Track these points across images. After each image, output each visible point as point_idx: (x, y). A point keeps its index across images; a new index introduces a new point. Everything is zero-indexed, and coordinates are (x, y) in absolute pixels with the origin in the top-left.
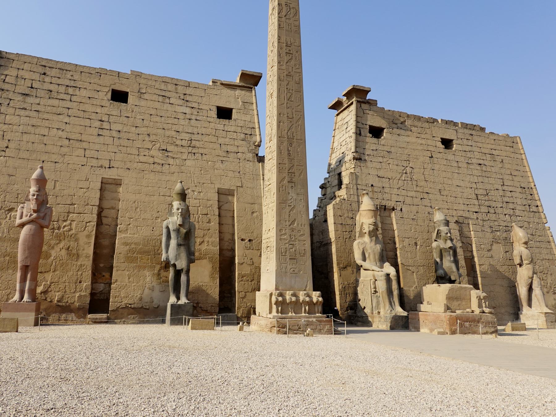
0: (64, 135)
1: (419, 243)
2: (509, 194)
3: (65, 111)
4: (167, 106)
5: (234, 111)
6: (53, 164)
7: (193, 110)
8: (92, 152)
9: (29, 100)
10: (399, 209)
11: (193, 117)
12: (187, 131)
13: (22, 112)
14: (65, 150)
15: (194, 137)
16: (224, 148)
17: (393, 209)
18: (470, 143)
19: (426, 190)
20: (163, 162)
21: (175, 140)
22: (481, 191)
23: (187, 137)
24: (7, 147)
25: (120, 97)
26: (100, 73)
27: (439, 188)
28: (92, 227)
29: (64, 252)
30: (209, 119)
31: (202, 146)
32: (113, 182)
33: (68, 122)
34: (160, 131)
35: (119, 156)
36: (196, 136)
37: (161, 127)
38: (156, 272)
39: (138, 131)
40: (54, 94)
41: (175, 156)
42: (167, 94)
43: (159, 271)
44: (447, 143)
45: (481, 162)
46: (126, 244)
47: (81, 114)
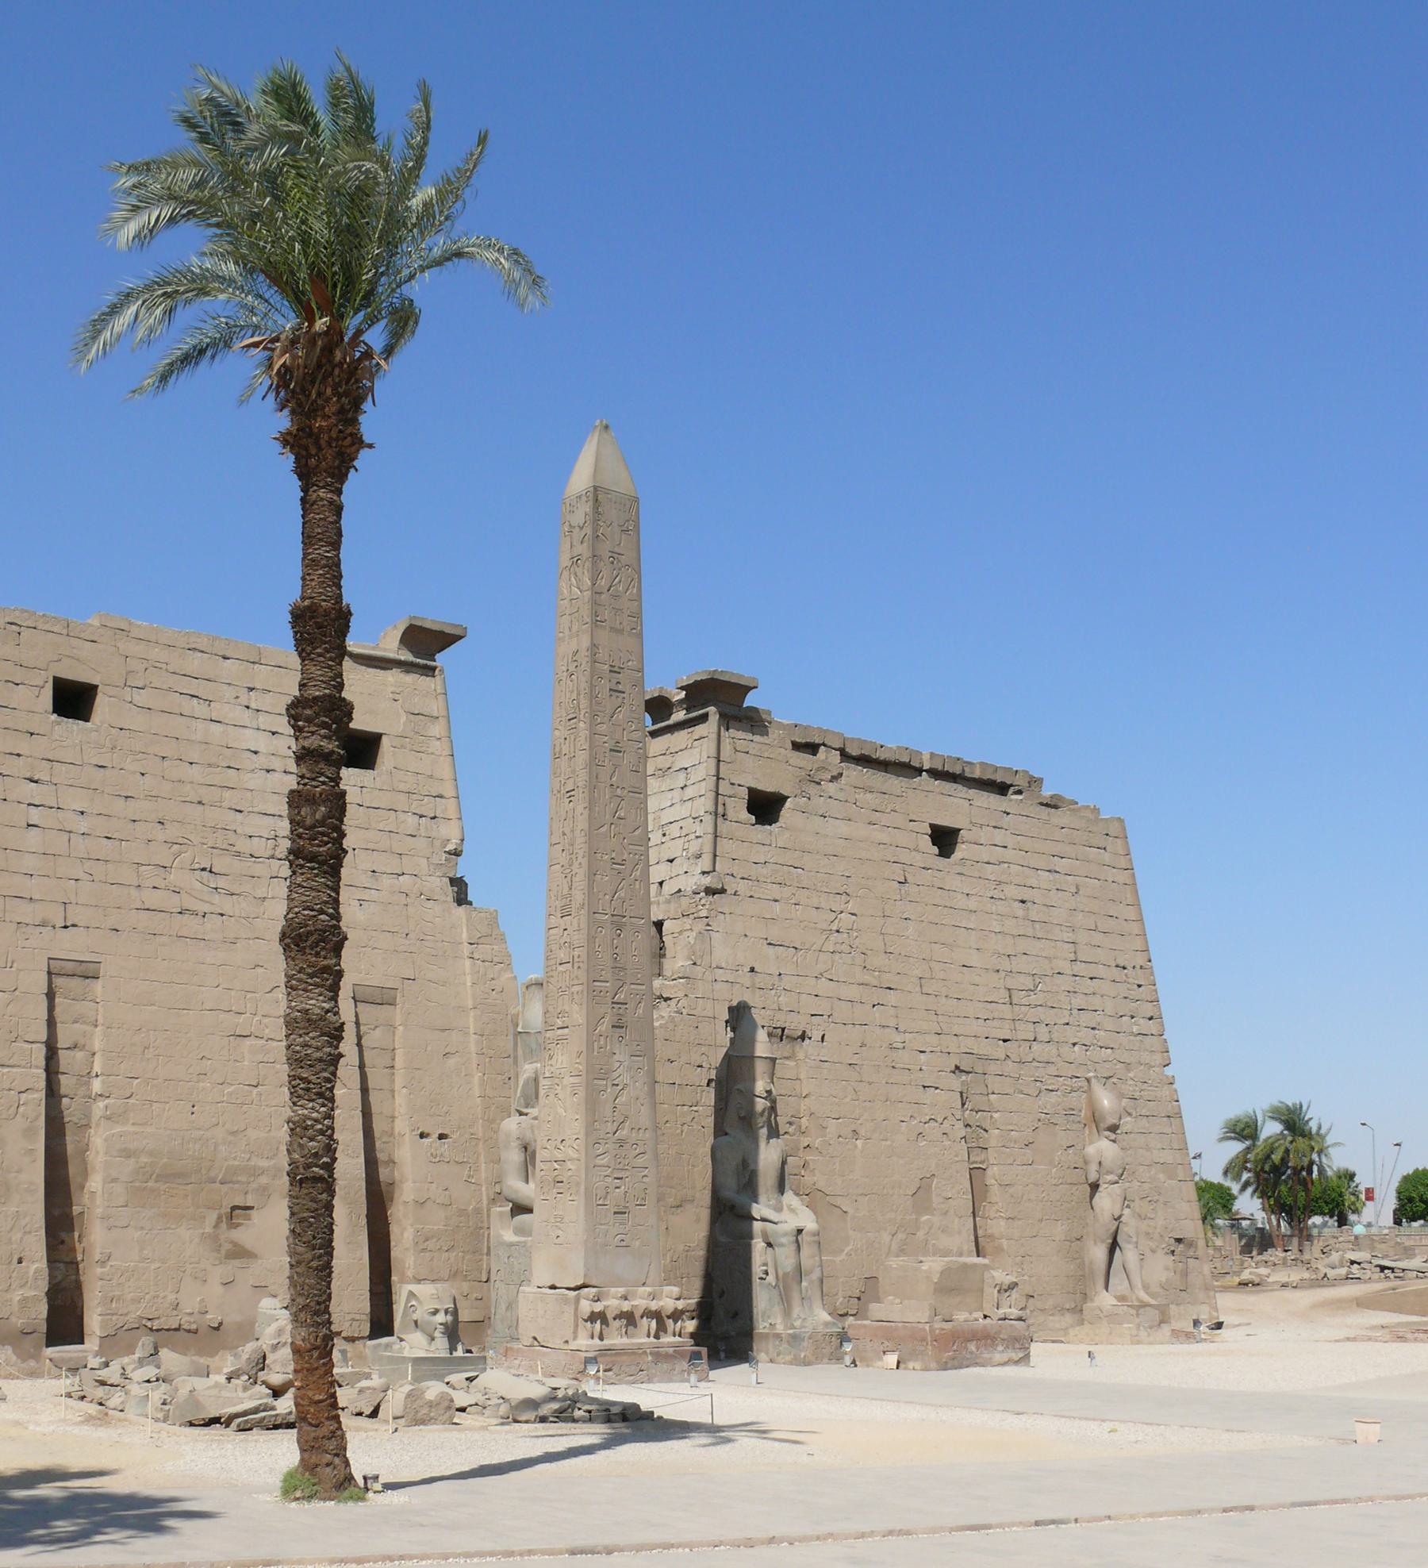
1: (862, 1132)
5: (385, 740)
10: (816, 1035)
17: (803, 1037)
19: (888, 979)
20: (206, 908)
21: (232, 838)
22: (1022, 978)
27: (918, 973)
32: (80, 969)
38: (209, 1229)
41: (234, 889)
43: (216, 1226)
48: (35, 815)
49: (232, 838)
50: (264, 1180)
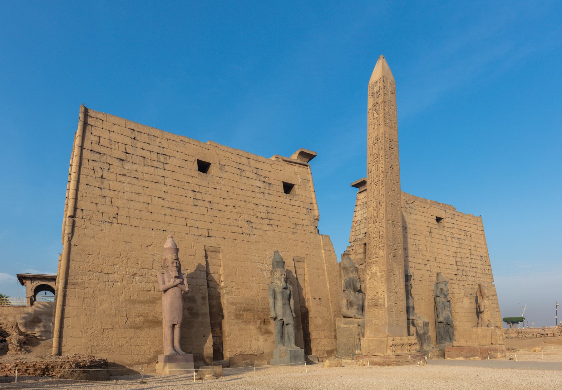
2: (473, 261)
4: (244, 180)
7: (265, 184)
8: (192, 221)
11: (266, 191)
12: (262, 204)
14: (168, 219)
15: (270, 210)
18: (453, 221)
20: (250, 232)
21: (255, 213)
23: (264, 209)
31: (276, 218)
33: (166, 191)
36: (271, 209)
37: (242, 199)
41: (258, 227)
45: (459, 236)
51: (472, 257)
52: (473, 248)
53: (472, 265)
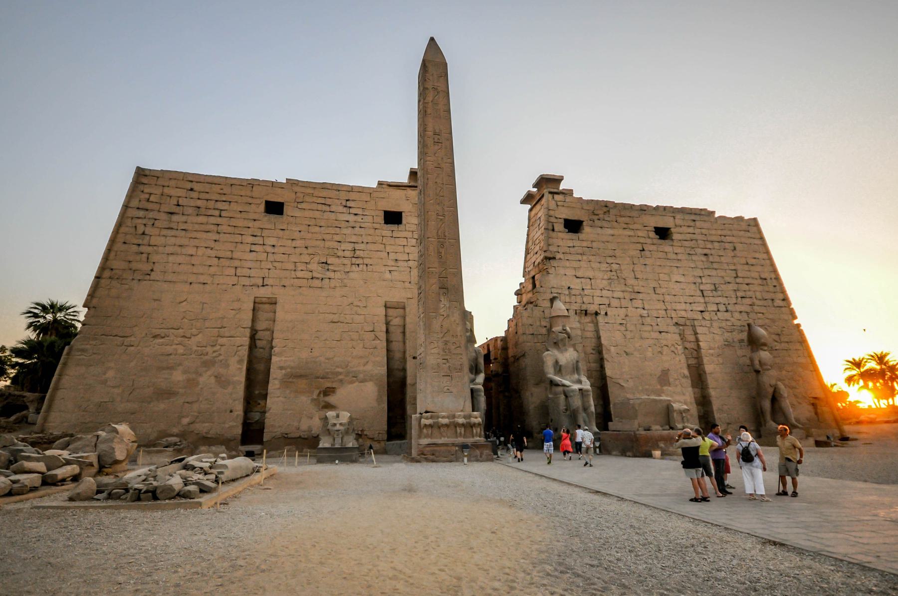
0: (213, 253)
3: (214, 228)
6: (201, 286)
9: (175, 218)
10: (603, 313)
11: (358, 225)
13: (170, 232)
15: (357, 246)
16: (393, 256)
17: (597, 314)
20: (323, 276)
21: (336, 251)
22: (708, 285)
23: (350, 247)
24: (152, 270)
25: (274, 208)
26: (252, 184)
27: (653, 286)
28: (244, 352)
29: (213, 380)
30: (376, 226)
34: (321, 243)
35: (273, 273)
38: (315, 397)
39: (294, 244)
40: (202, 211)
41: (336, 269)
42: (328, 202)
44: (663, 233)
45: (706, 251)
46: (281, 368)
47: (230, 230)
48: (254, 248)
49: (336, 251)
50: (341, 377)
51: (738, 280)
52: (739, 267)
53: (740, 294)
